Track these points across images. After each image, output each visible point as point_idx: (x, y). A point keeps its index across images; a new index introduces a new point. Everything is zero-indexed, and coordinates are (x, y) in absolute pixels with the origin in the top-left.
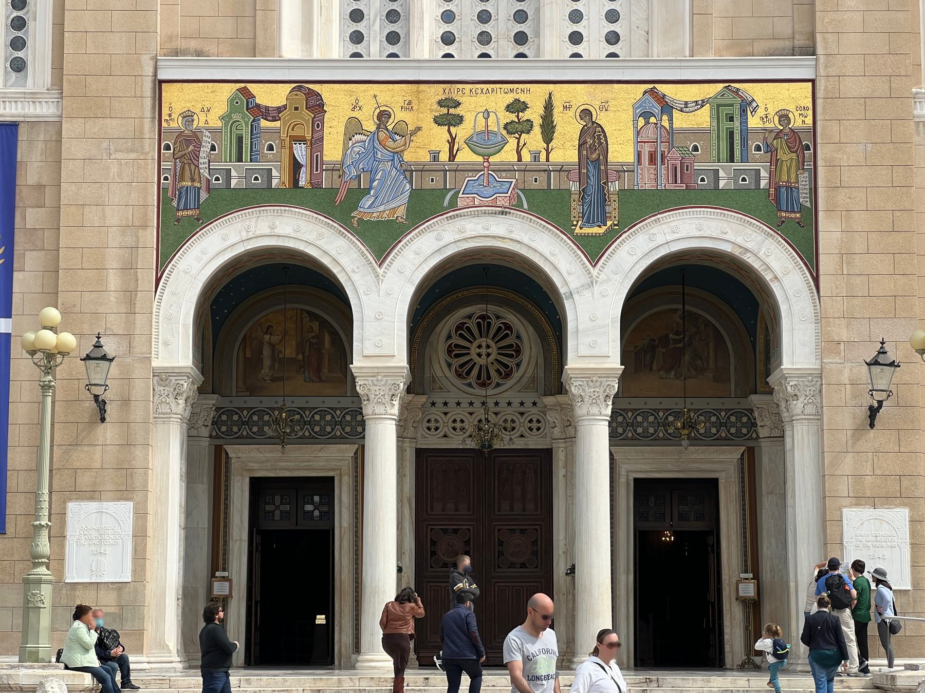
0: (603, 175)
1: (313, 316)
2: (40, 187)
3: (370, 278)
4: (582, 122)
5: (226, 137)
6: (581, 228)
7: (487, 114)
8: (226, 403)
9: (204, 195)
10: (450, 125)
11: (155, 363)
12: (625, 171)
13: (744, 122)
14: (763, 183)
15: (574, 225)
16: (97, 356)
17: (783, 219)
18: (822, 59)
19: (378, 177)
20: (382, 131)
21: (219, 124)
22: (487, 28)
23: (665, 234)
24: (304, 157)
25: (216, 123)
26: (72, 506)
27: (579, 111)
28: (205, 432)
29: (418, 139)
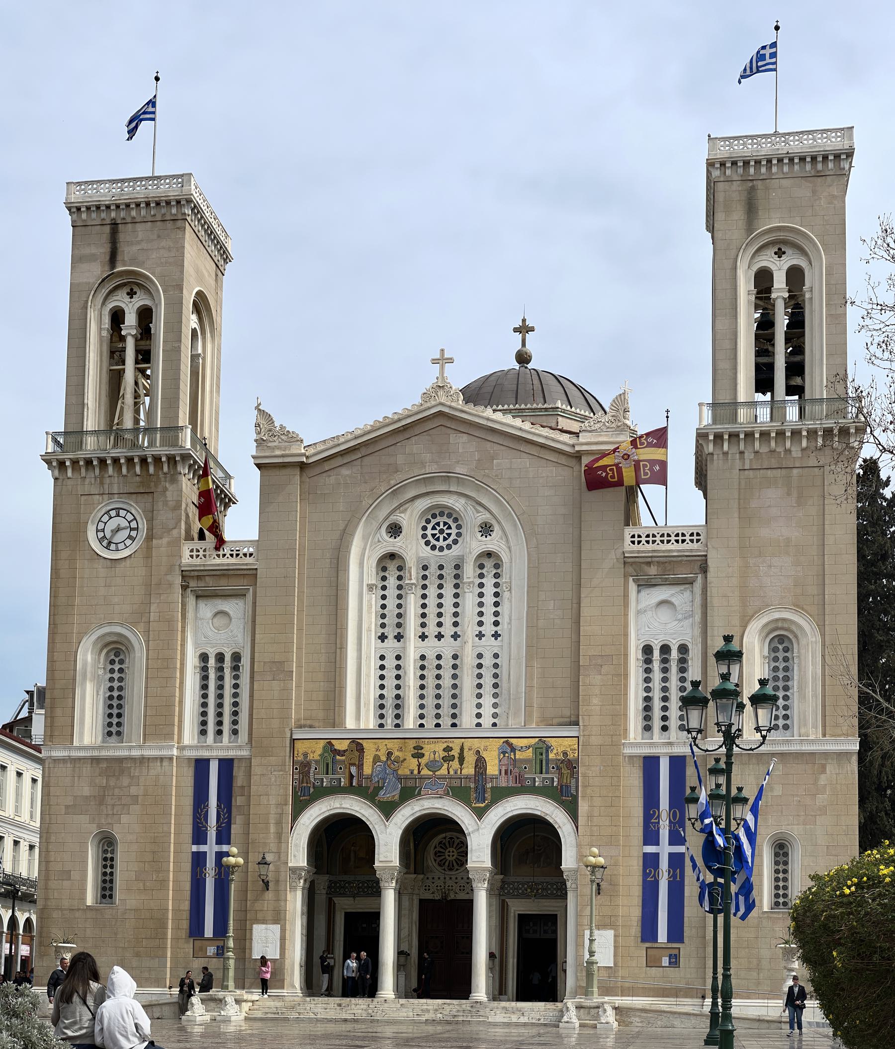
2: (243, 787)
3: (383, 827)
9: (312, 790)
10: (418, 757)
11: (290, 865)
13: (547, 756)
14: (555, 784)
16: (263, 862)
18: (581, 727)
21: (319, 758)
22: (439, 711)
25: (317, 757)
26: (254, 926)
28: (324, 892)
29: (405, 764)
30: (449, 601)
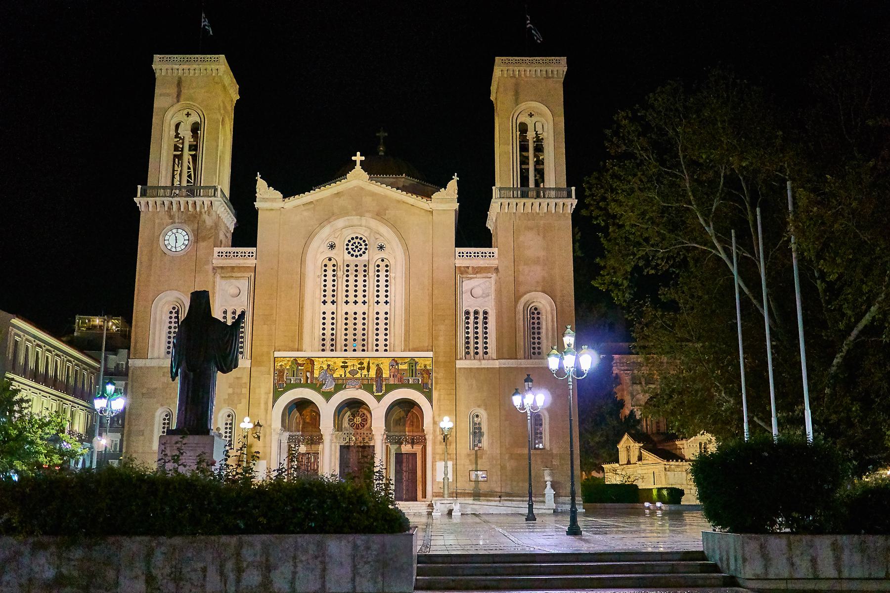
1: (314, 412)
2: (245, 383)
8: (291, 433)
9: (285, 385)
13: (416, 367)
30: (360, 283)
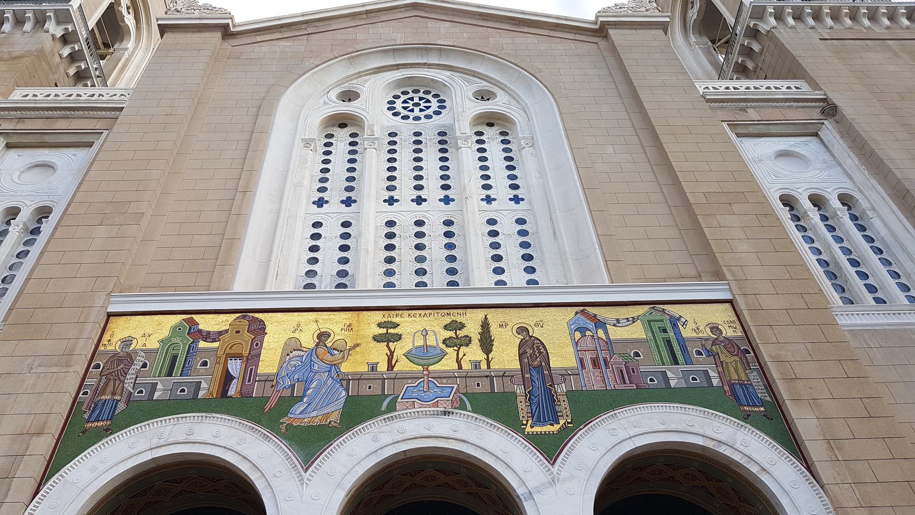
0: (547, 379)
4: (520, 336)
5: (160, 358)
6: (532, 427)
7: (425, 333)
9: (121, 406)
10: (388, 341)
12: (570, 375)
13: (678, 333)
14: (715, 382)
15: (523, 425)
17: (748, 413)
19: (313, 386)
20: (321, 347)
23: (626, 429)
24: (238, 370)
27: (517, 326)
29: (356, 356)
